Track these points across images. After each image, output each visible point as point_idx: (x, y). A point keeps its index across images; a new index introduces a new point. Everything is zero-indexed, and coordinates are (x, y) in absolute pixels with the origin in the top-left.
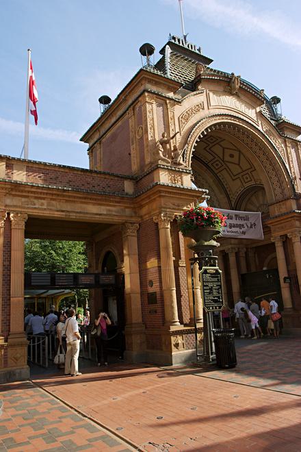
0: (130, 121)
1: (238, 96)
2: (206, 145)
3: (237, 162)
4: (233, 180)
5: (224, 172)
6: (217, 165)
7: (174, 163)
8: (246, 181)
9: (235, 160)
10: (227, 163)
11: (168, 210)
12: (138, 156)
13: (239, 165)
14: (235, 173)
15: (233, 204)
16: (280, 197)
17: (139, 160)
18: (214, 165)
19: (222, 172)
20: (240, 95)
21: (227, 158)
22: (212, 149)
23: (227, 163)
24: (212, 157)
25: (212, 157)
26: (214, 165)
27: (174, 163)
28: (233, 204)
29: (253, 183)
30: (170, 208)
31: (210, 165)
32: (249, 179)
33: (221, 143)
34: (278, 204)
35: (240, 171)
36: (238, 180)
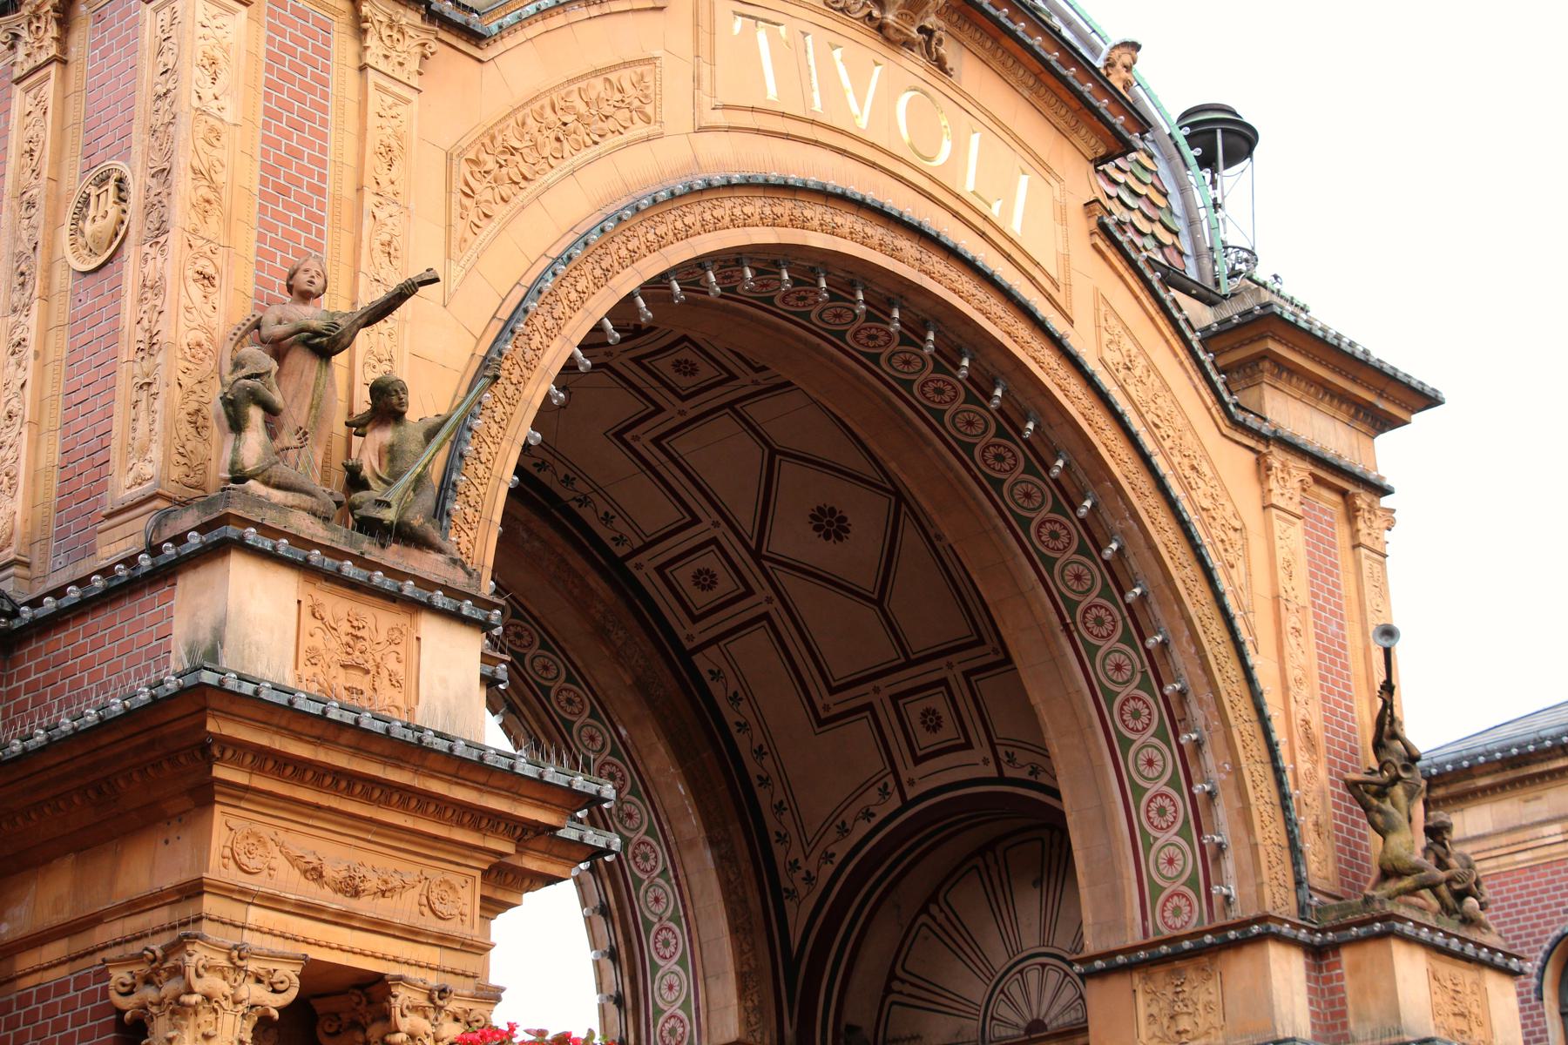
0: (20, 101)
1: (940, 64)
2: (632, 406)
3: (868, 583)
4: (822, 722)
5: (755, 650)
6: (705, 580)
7: (369, 526)
8: (925, 740)
9: (856, 555)
10: (781, 575)
11: (255, 915)
12: (54, 417)
13: (879, 603)
14: (840, 671)
15: (798, 916)
16: (1187, 918)
17: (51, 453)
18: (683, 575)
19: (736, 646)
20: (949, 50)
21: (792, 537)
22: (682, 445)
23: (781, 575)
24: (670, 514)
25: (670, 514)
27: (369, 526)
28: (798, 916)
29: (975, 764)
30: (273, 902)
31: (644, 569)
32: (949, 731)
33: (757, 411)
34: (1160, 974)
35: (883, 650)
36: (861, 729)
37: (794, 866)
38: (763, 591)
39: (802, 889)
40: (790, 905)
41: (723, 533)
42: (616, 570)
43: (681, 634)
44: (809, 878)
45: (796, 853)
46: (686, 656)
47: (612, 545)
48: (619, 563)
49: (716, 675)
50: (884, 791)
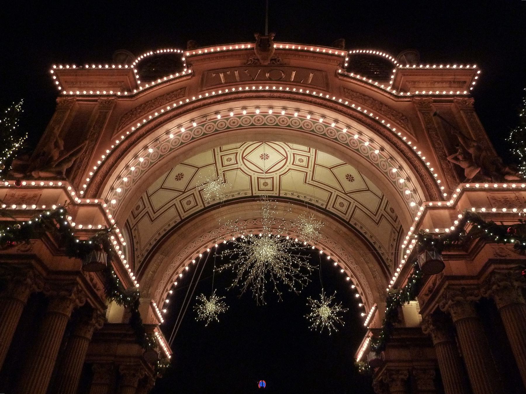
2: (303, 175)
25: (327, 194)
26: (337, 206)
31: (330, 208)
37: (387, 259)
38: (352, 201)
39: (390, 263)
40: (390, 269)
41: (337, 193)
43: (345, 219)
44: (391, 261)
45: (387, 256)
46: (348, 223)
47: (321, 206)
48: (325, 210)
49: (355, 224)
50: (394, 233)
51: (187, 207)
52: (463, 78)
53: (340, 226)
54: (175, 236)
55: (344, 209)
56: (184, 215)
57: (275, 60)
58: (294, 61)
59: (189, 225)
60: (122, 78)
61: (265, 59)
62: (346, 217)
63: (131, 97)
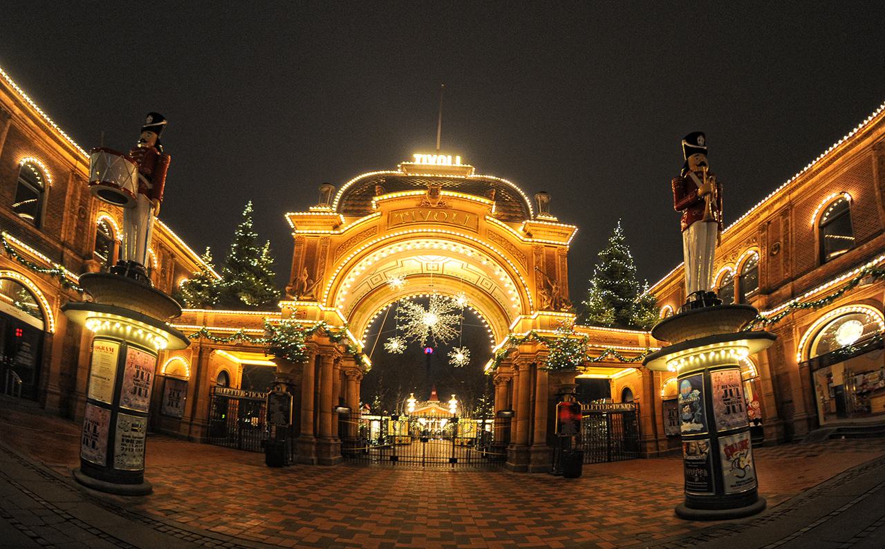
25: (478, 277)
26: (484, 284)
31: (479, 284)
42: (475, 287)
51: (375, 282)
52: (567, 232)
53: (484, 296)
54: (368, 300)
55: (488, 287)
56: (373, 287)
57: (442, 203)
58: (455, 204)
59: (377, 293)
60: (331, 220)
61: (434, 204)
62: (490, 292)
63: (341, 234)
